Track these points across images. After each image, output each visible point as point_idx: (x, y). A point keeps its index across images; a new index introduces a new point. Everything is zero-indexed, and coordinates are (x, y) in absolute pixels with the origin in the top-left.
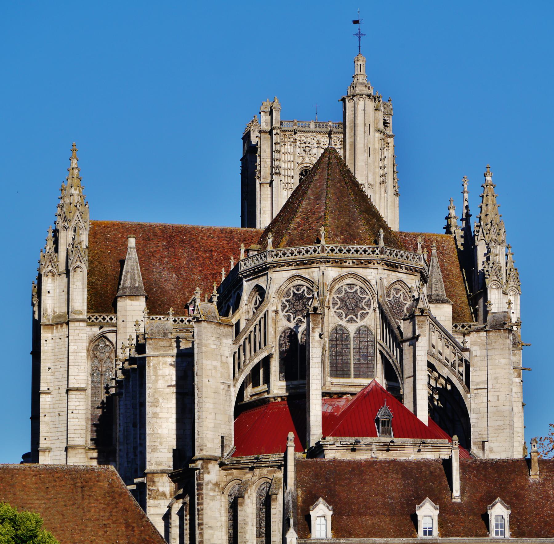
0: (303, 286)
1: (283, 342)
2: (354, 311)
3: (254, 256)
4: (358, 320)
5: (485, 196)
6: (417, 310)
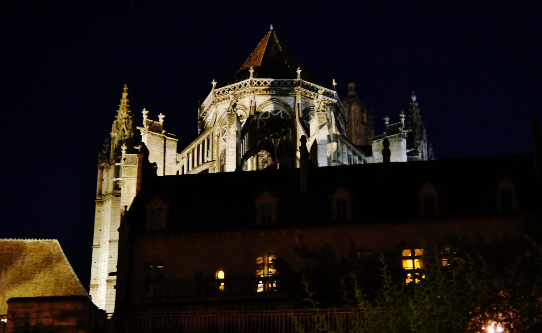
1: (223, 158)
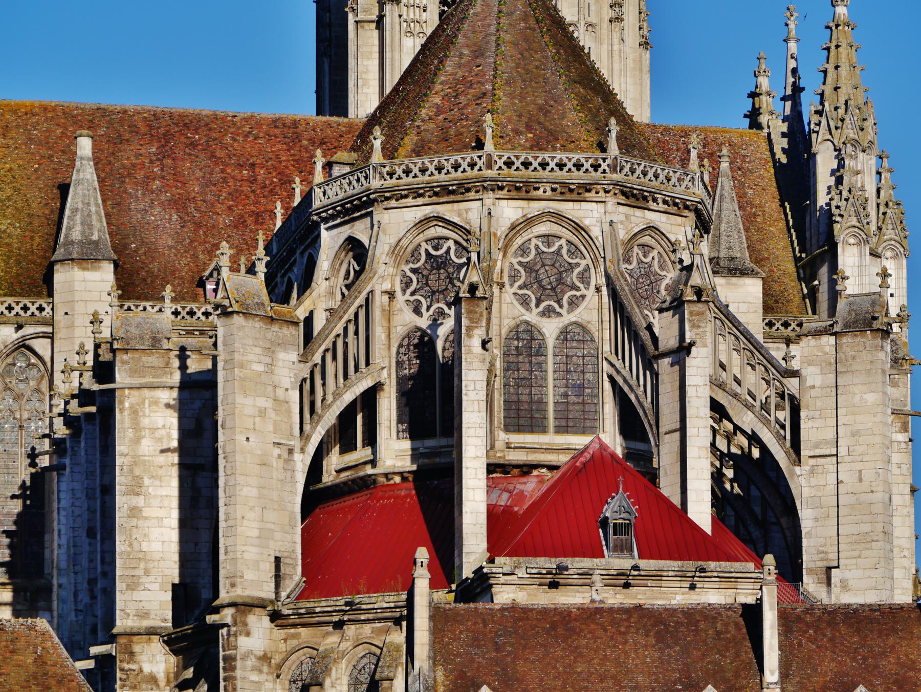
0: (447, 239)
1: (405, 358)
2: (555, 292)
3: (343, 176)
4: (564, 311)
5: (833, 48)
6: (689, 289)
